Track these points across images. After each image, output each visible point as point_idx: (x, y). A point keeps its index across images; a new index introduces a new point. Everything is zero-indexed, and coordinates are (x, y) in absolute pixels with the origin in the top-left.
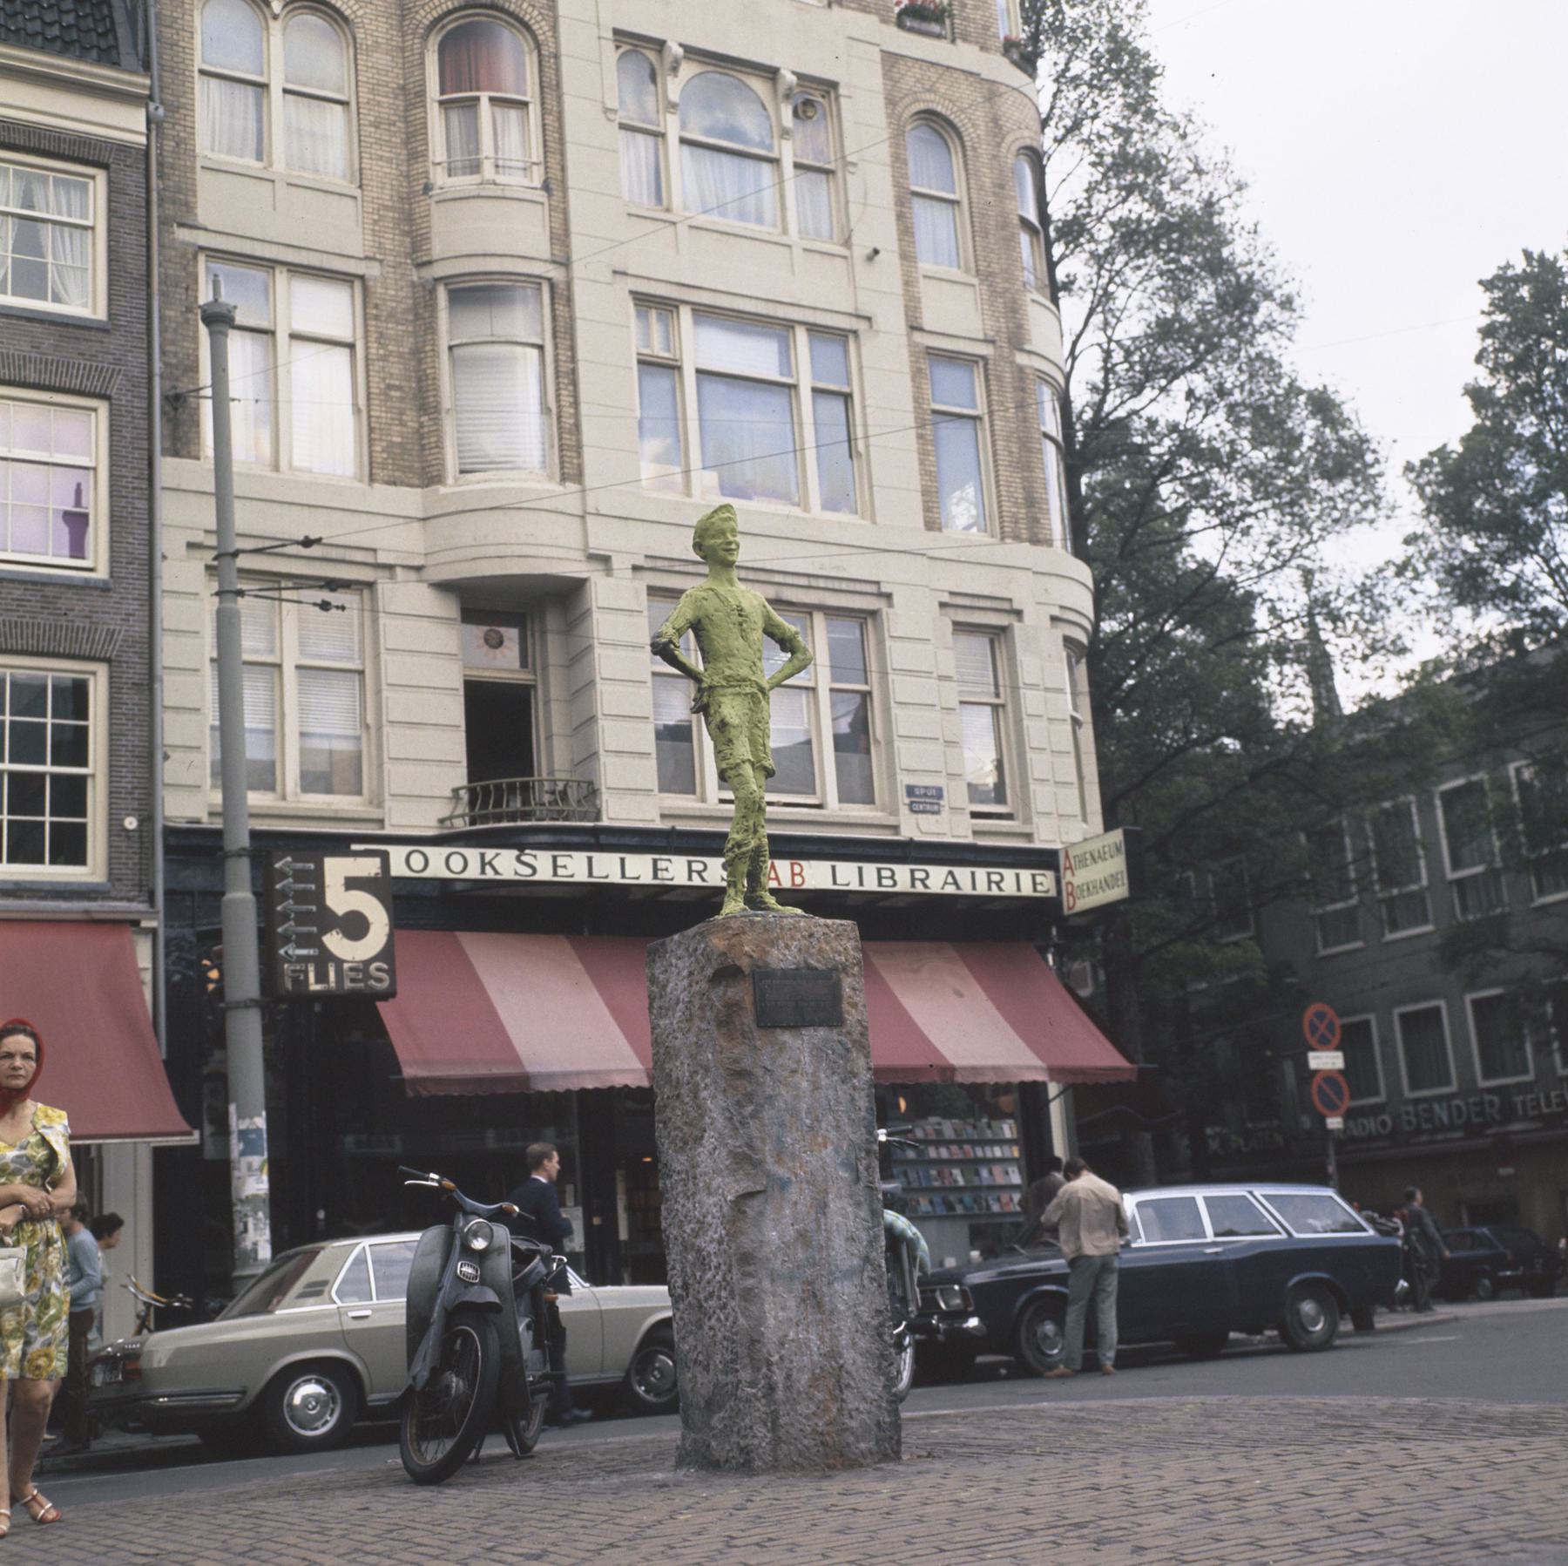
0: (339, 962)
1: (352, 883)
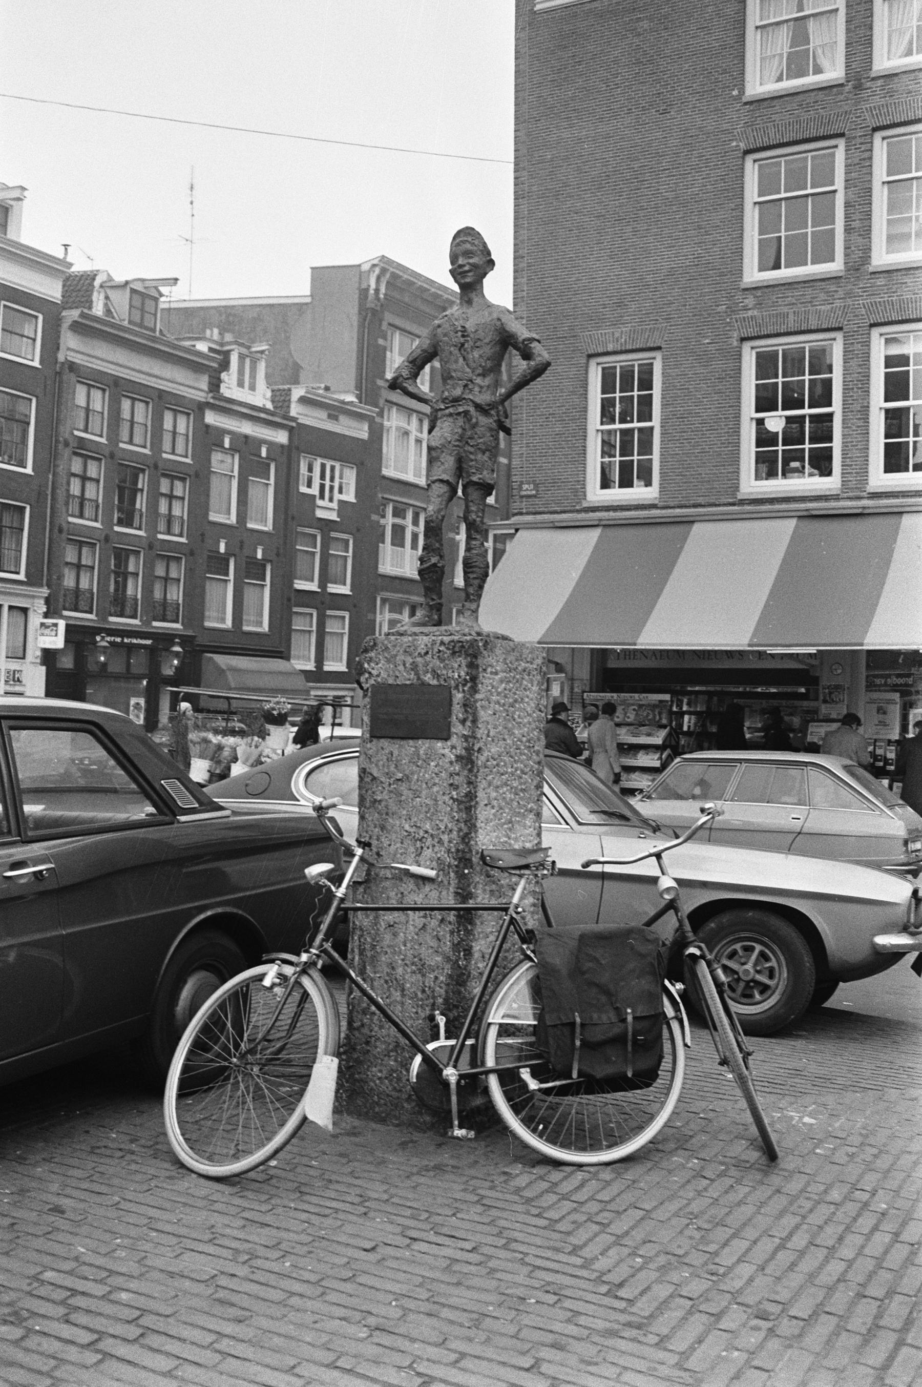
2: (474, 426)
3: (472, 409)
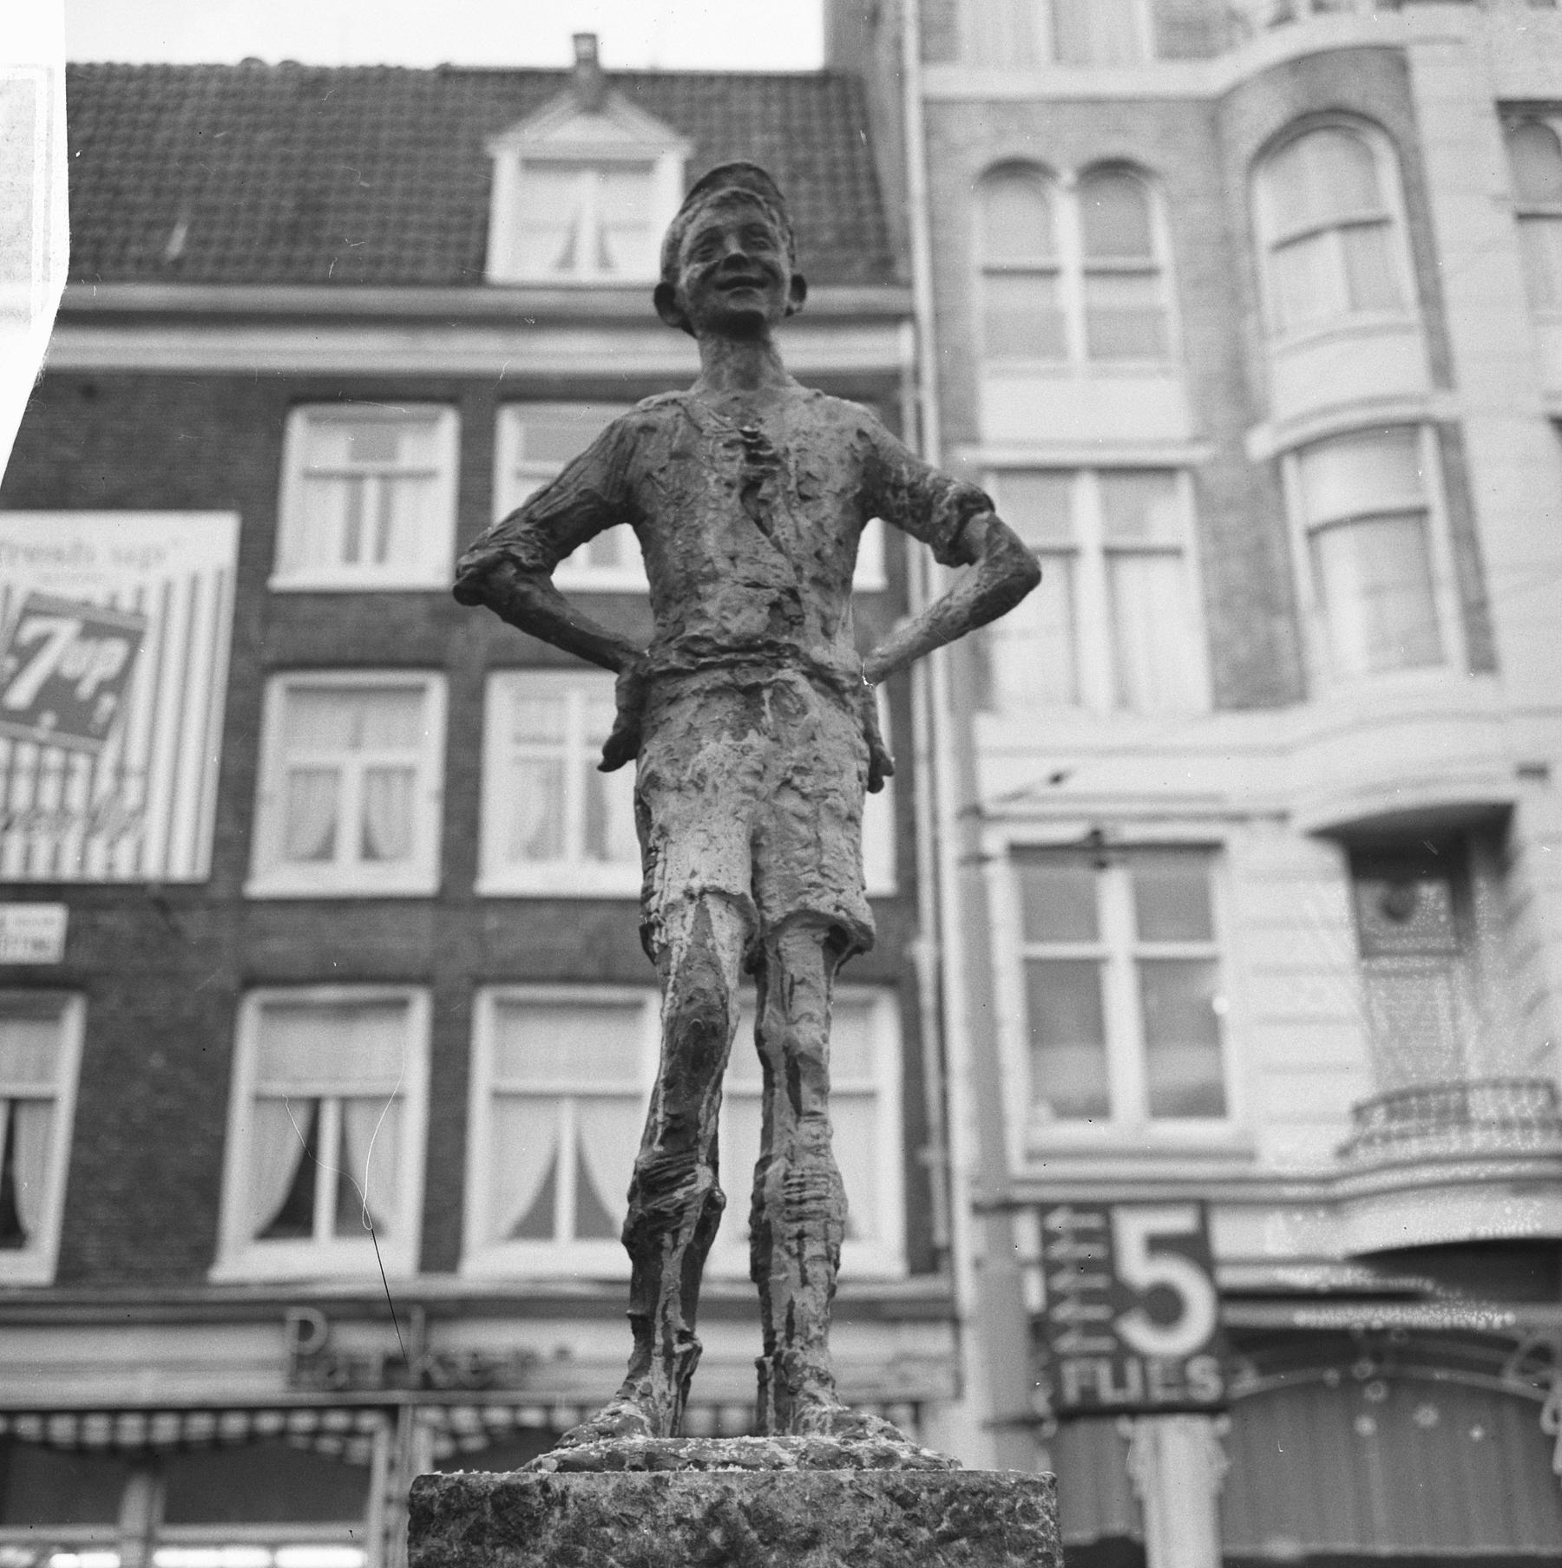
0: (1143, 1359)
1: (1158, 1245)
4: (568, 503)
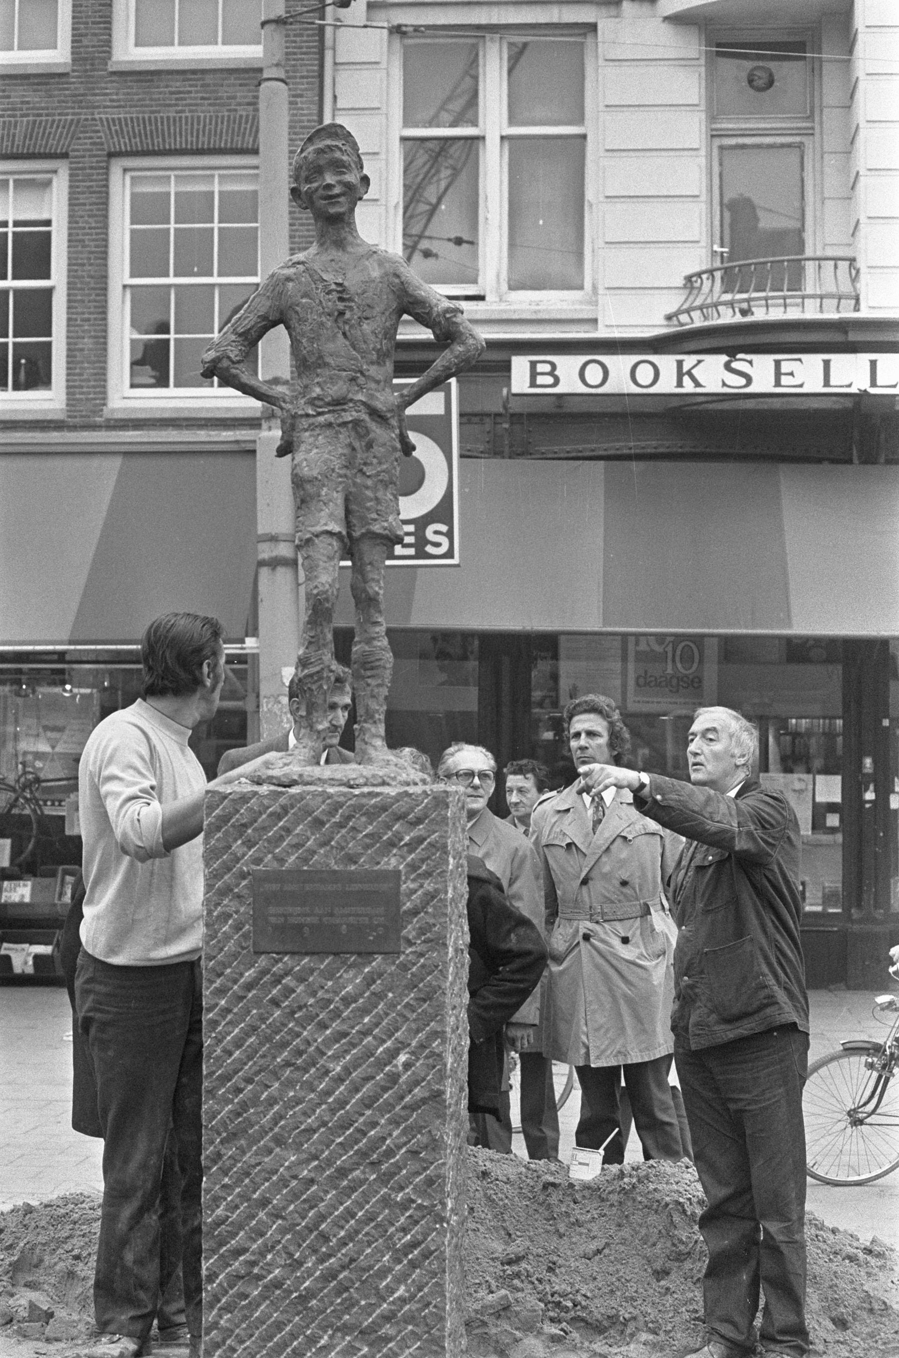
2: (369, 446)
3: (366, 418)
4: (252, 323)
